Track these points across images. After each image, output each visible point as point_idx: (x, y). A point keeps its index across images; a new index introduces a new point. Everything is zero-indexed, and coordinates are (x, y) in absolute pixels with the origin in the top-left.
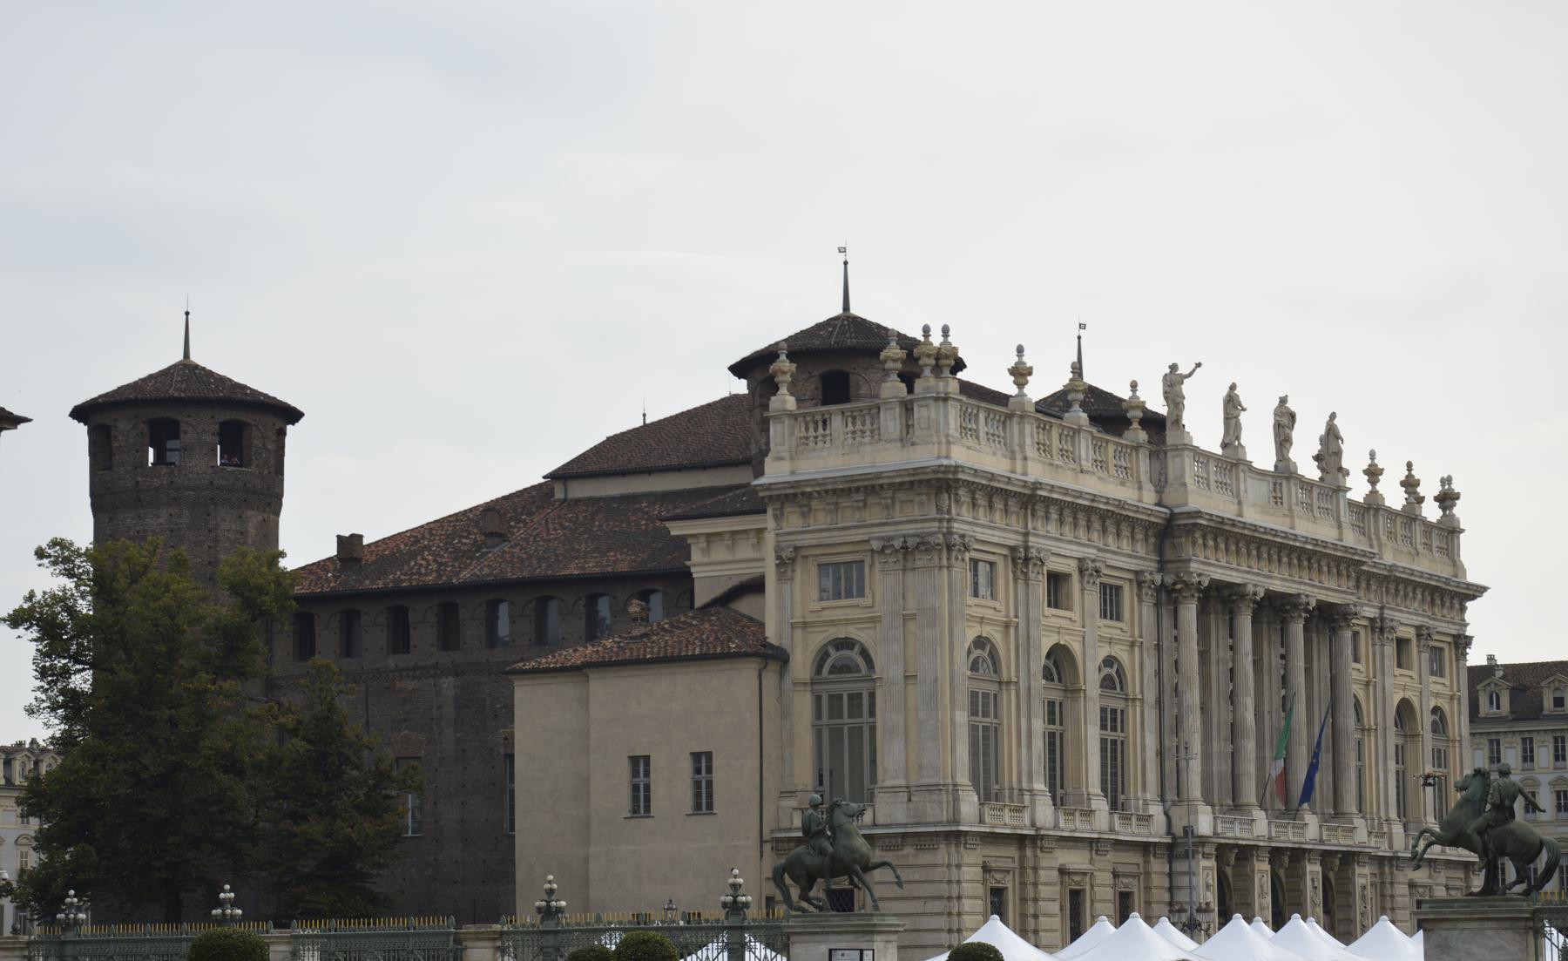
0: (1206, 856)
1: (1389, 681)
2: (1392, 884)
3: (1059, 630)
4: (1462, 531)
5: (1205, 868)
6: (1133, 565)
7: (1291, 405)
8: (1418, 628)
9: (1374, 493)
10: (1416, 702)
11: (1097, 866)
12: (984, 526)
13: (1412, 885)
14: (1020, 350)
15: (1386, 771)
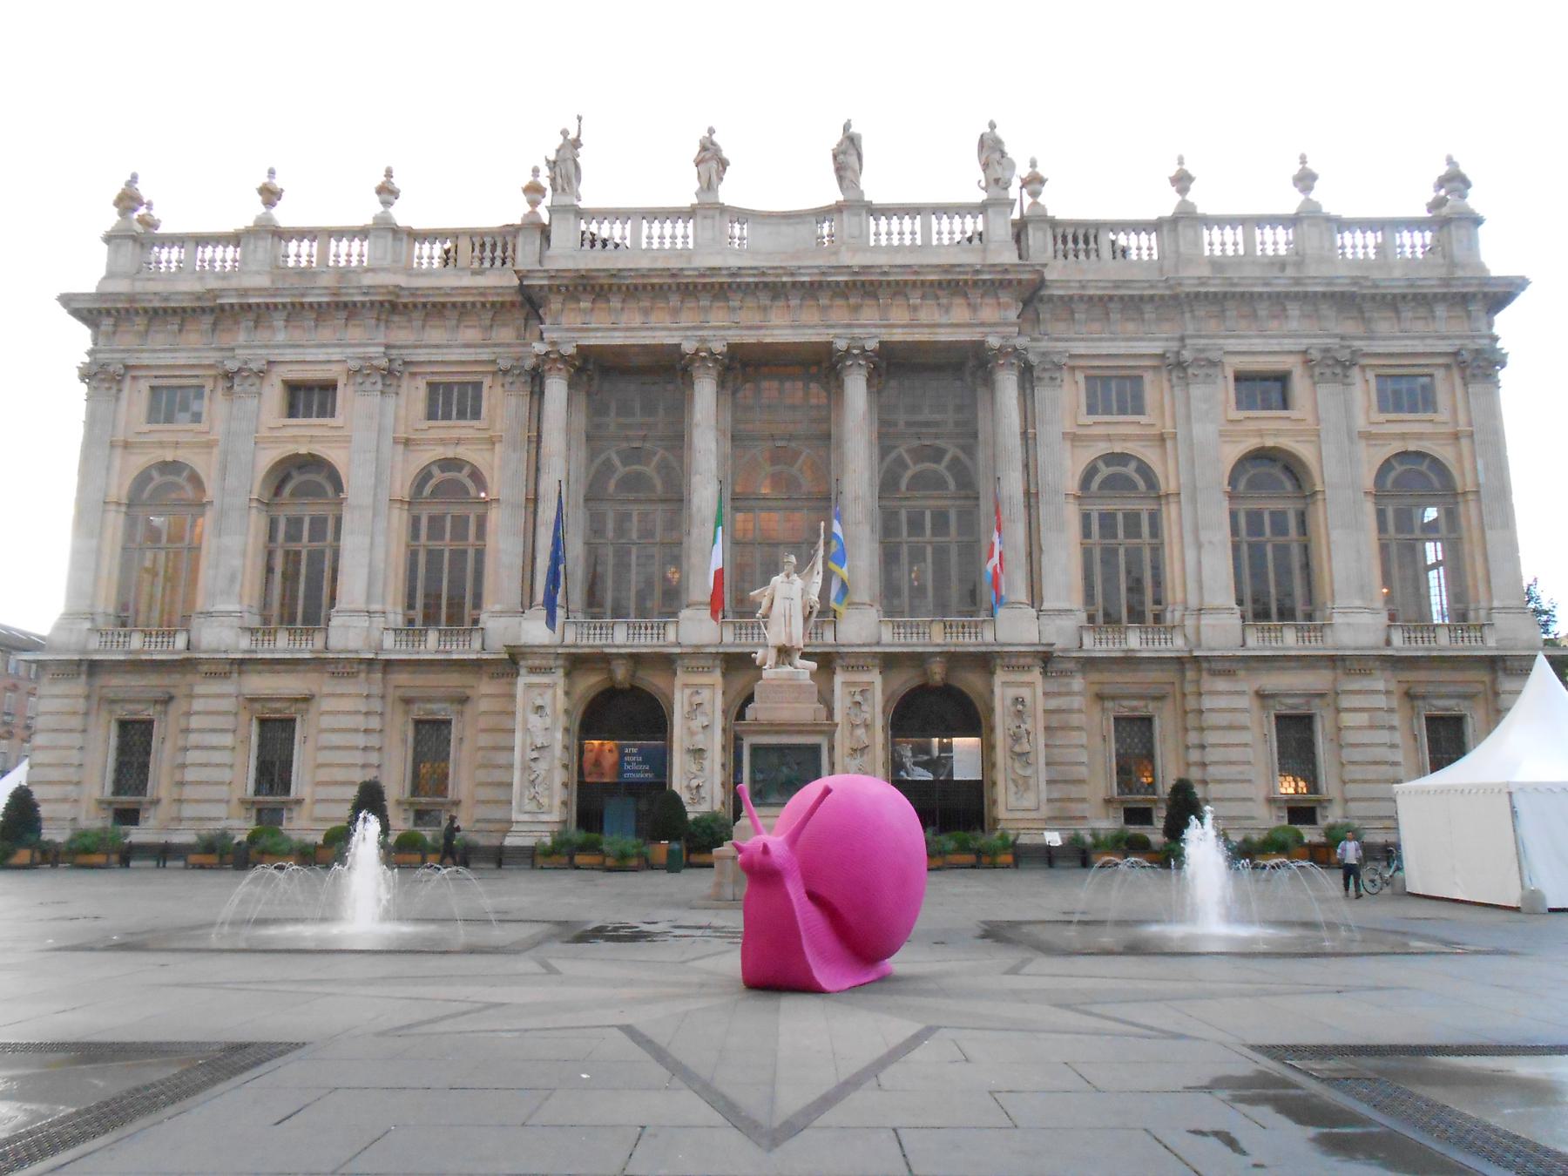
0: (533, 670)
1: (1204, 432)
2: (1200, 694)
3: (294, 439)
4: (1478, 221)
5: (529, 686)
6: (485, 355)
7: (854, 130)
8: (1305, 352)
9: (1184, 202)
10: (1305, 451)
11: (326, 690)
12: (155, 351)
13: (1262, 696)
14: (272, 173)
15: (1199, 546)
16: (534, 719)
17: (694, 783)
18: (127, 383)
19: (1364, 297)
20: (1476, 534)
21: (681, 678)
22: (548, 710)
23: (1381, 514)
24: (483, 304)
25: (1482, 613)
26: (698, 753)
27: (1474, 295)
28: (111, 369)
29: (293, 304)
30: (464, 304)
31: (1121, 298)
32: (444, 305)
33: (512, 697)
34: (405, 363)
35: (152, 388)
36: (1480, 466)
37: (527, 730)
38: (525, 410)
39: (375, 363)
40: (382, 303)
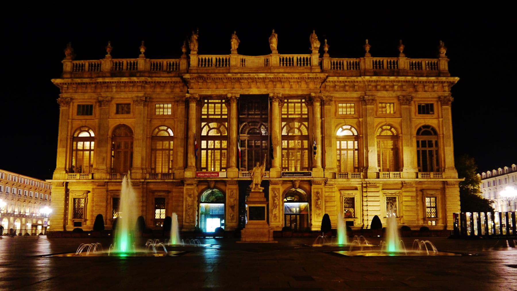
0: (188, 185)
5: (187, 189)
16: (188, 198)
17: (232, 215)
18: (71, 104)
19: (415, 82)
20: (442, 147)
21: (228, 186)
22: (192, 196)
23: (418, 142)
24: (171, 82)
25: (443, 169)
26: (232, 207)
27: (445, 82)
28: (67, 100)
29: (118, 82)
30: (166, 82)
31: (349, 82)
32: (160, 82)
33: (183, 193)
34: (150, 98)
35: (78, 105)
36: (444, 129)
37: (186, 201)
38: (183, 112)
39: (142, 98)
40: (143, 82)
